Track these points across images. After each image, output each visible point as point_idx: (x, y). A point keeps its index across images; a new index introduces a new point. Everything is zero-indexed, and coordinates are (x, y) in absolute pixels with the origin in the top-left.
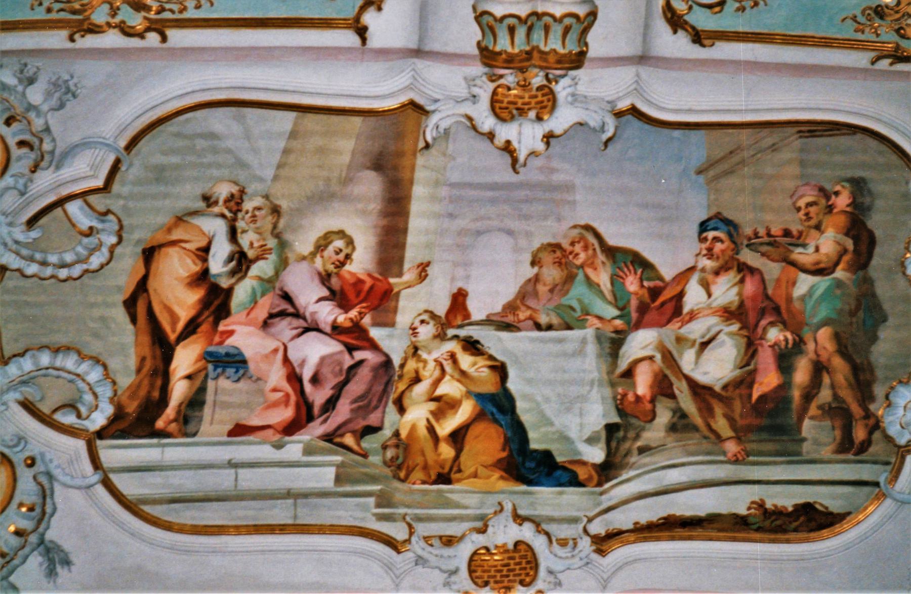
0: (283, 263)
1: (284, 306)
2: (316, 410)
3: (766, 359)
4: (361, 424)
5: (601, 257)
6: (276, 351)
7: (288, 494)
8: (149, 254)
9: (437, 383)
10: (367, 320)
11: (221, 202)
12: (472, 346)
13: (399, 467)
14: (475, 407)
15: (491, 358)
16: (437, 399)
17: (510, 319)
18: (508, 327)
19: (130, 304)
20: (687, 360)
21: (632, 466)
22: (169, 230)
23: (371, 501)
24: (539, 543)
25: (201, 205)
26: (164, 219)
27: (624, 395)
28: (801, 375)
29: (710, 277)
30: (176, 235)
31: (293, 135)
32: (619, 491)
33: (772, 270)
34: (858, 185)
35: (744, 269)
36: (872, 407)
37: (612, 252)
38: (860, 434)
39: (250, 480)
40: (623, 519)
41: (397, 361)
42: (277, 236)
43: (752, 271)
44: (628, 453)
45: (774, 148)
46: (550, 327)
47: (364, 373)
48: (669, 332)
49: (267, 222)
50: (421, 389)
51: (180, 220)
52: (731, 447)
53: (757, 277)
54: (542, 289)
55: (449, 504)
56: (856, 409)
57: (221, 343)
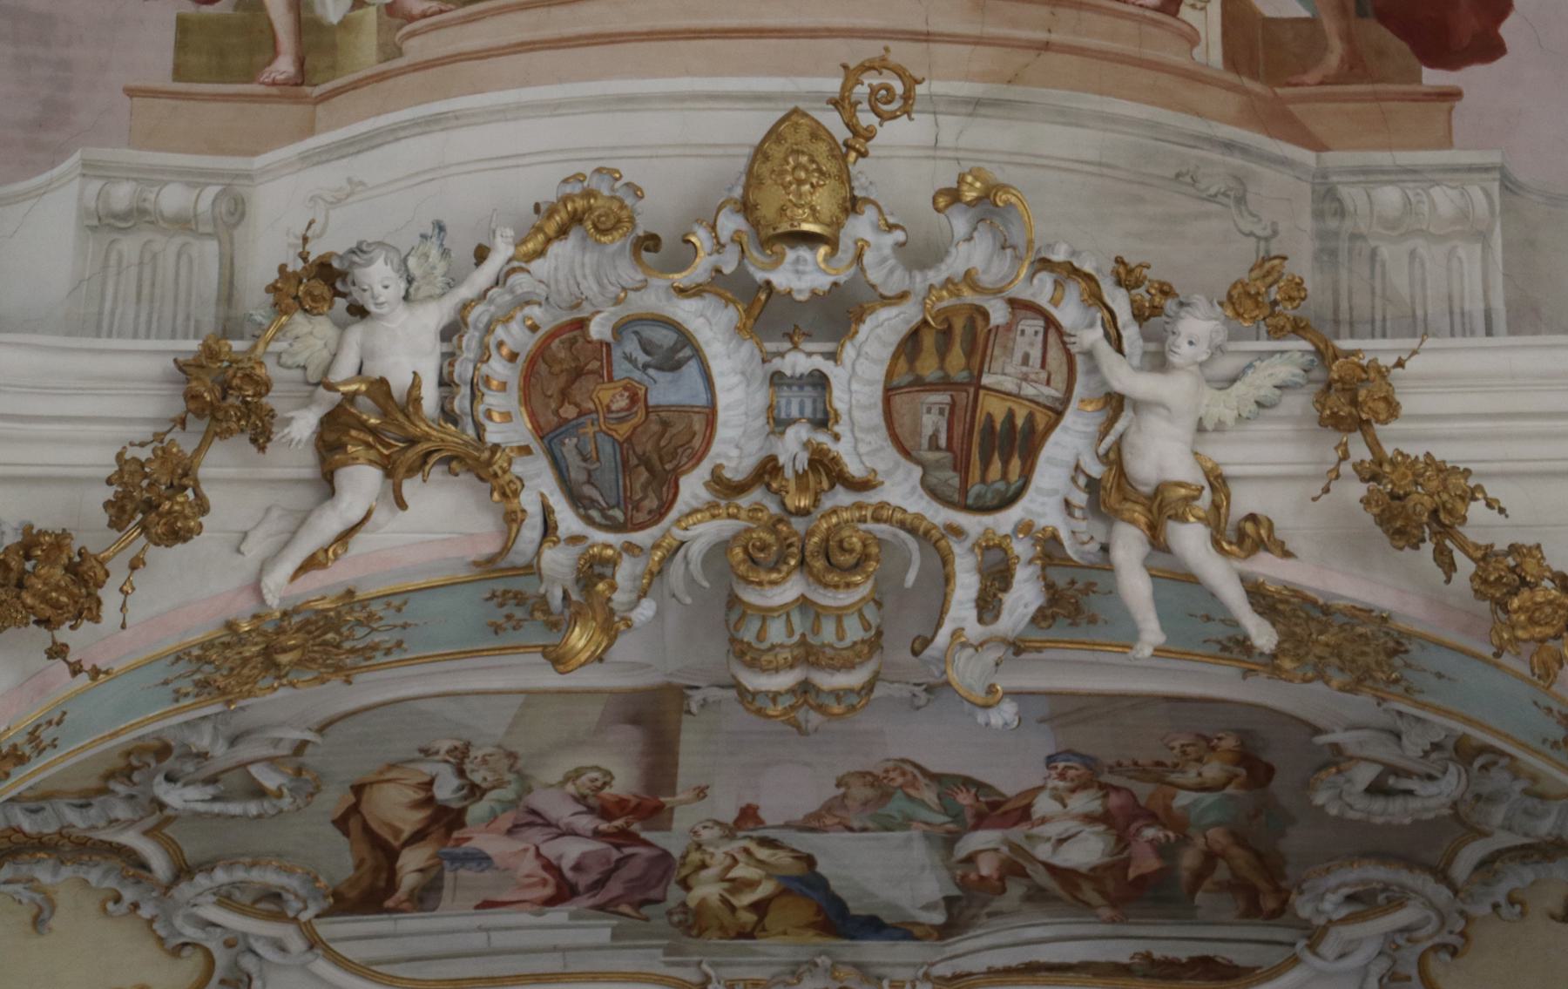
5: (922, 780)
7: (555, 949)
8: (358, 789)
11: (442, 752)
13: (690, 928)
15: (793, 850)
16: (732, 880)
18: (813, 830)
21: (980, 927)
23: (660, 951)
25: (417, 755)
27: (964, 877)
28: (1189, 859)
44: (975, 916)
46: (864, 830)
48: (1017, 833)
52: (1106, 912)
55: (754, 953)
56: (1262, 885)
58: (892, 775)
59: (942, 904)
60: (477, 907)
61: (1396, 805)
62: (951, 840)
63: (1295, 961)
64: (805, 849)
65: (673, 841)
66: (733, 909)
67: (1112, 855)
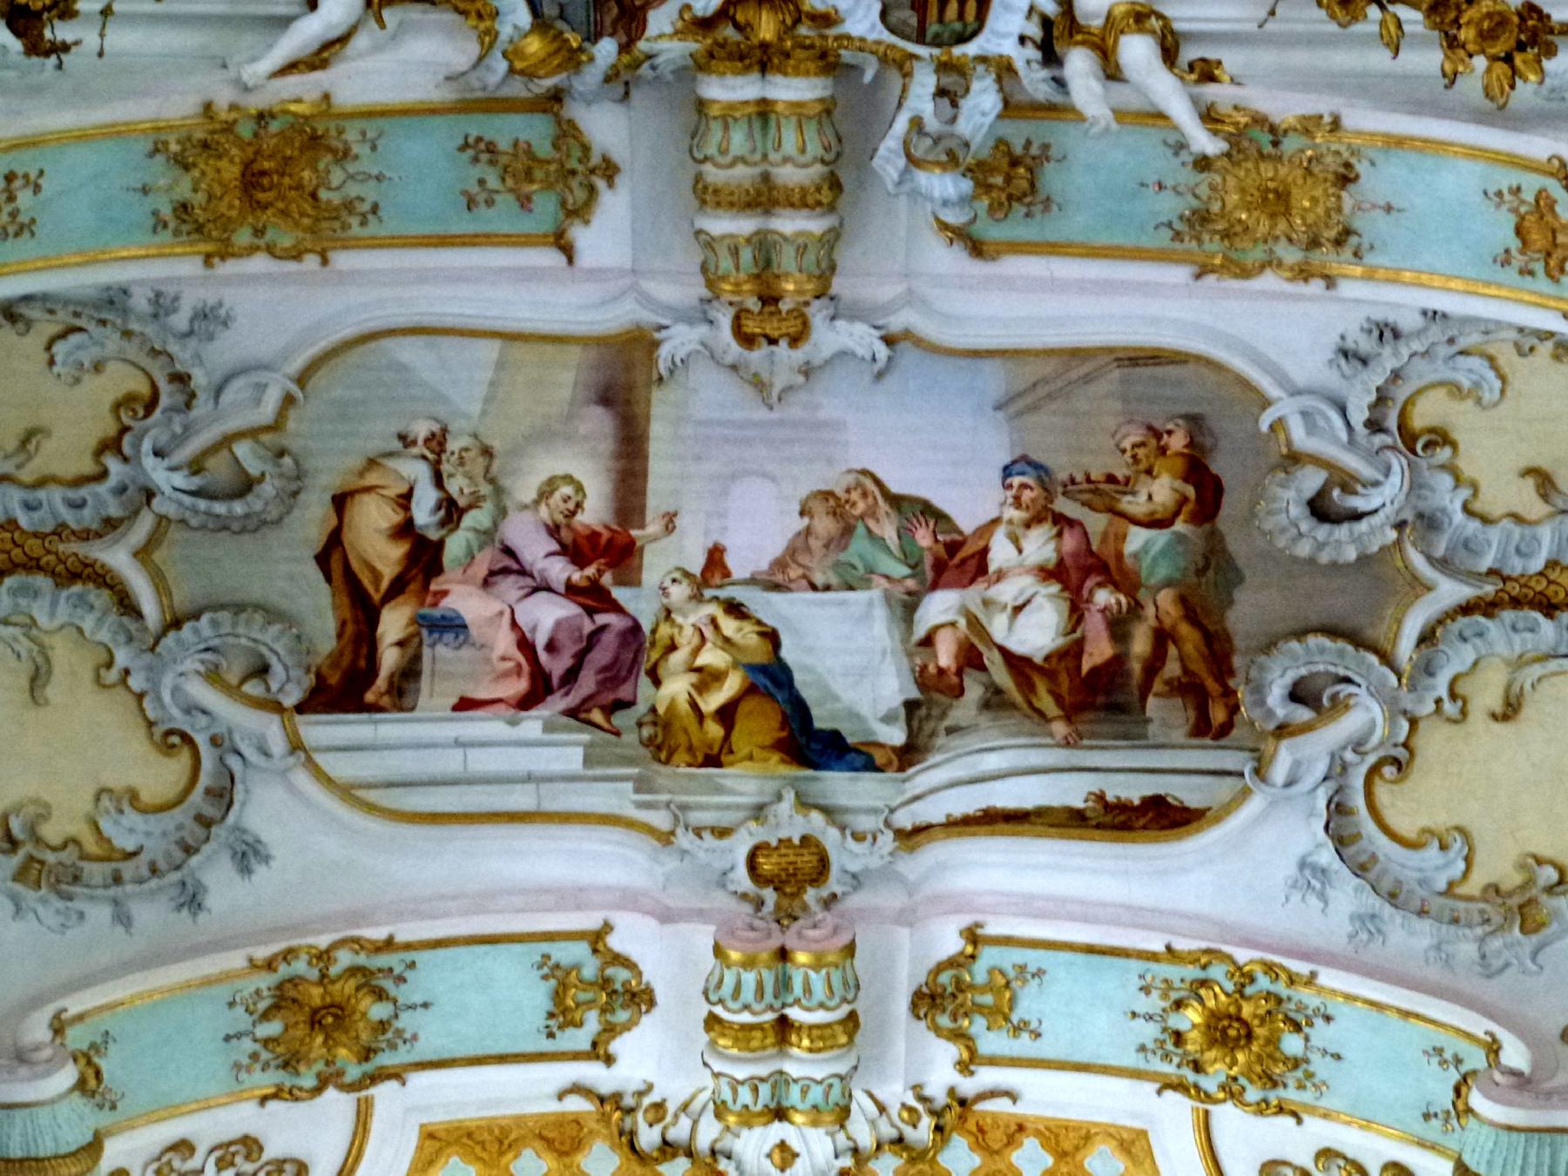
0: (502, 512)
1: (508, 562)
2: (555, 681)
3: (1095, 625)
4: (608, 697)
6: (501, 613)
7: (529, 778)
8: (341, 502)
9: (696, 652)
10: (607, 579)
11: (420, 442)
12: (735, 609)
13: (659, 748)
14: (744, 679)
15: (759, 623)
16: (699, 670)
17: (779, 578)
18: (777, 587)
19: (323, 559)
20: (998, 627)
21: (940, 749)
22: (361, 474)
23: (629, 786)
24: (830, 838)
25: (397, 445)
26: (357, 462)
27: (924, 668)
28: (1140, 644)
29: (1020, 531)
30: (372, 479)
31: (500, 365)
32: (923, 778)
33: (1096, 523)
34: (1195, 422)
35: (1061, 521)
36: (1232, 683)
37: (896, 501)
38: (1218, 715)
39: (483, 762)
40: (934, 811)
41: (646, 627)
42: (492, 481)
43: (1071, 523)
44: (933, 734)
45: (1087, 379)
46: (827, 588)
47: (609, 639)
48: (972, 596)
49: (477, 464)
50: (678, 658)
51: (372, 463)
52: (1060, 728)
53: (1077, 530)
54: (815, 544)
55: (720, 790)
56: (1211, 685)
57: (435, 605)
58: (855, 496)
59: (902, 712)
60: (456, 708)
61: (1343, 531)
62: (908, 608)
63: (1245, 793)
64: (770, 621)
65: (639, 603)
66: (700, 716)
67: (1066, 634)
